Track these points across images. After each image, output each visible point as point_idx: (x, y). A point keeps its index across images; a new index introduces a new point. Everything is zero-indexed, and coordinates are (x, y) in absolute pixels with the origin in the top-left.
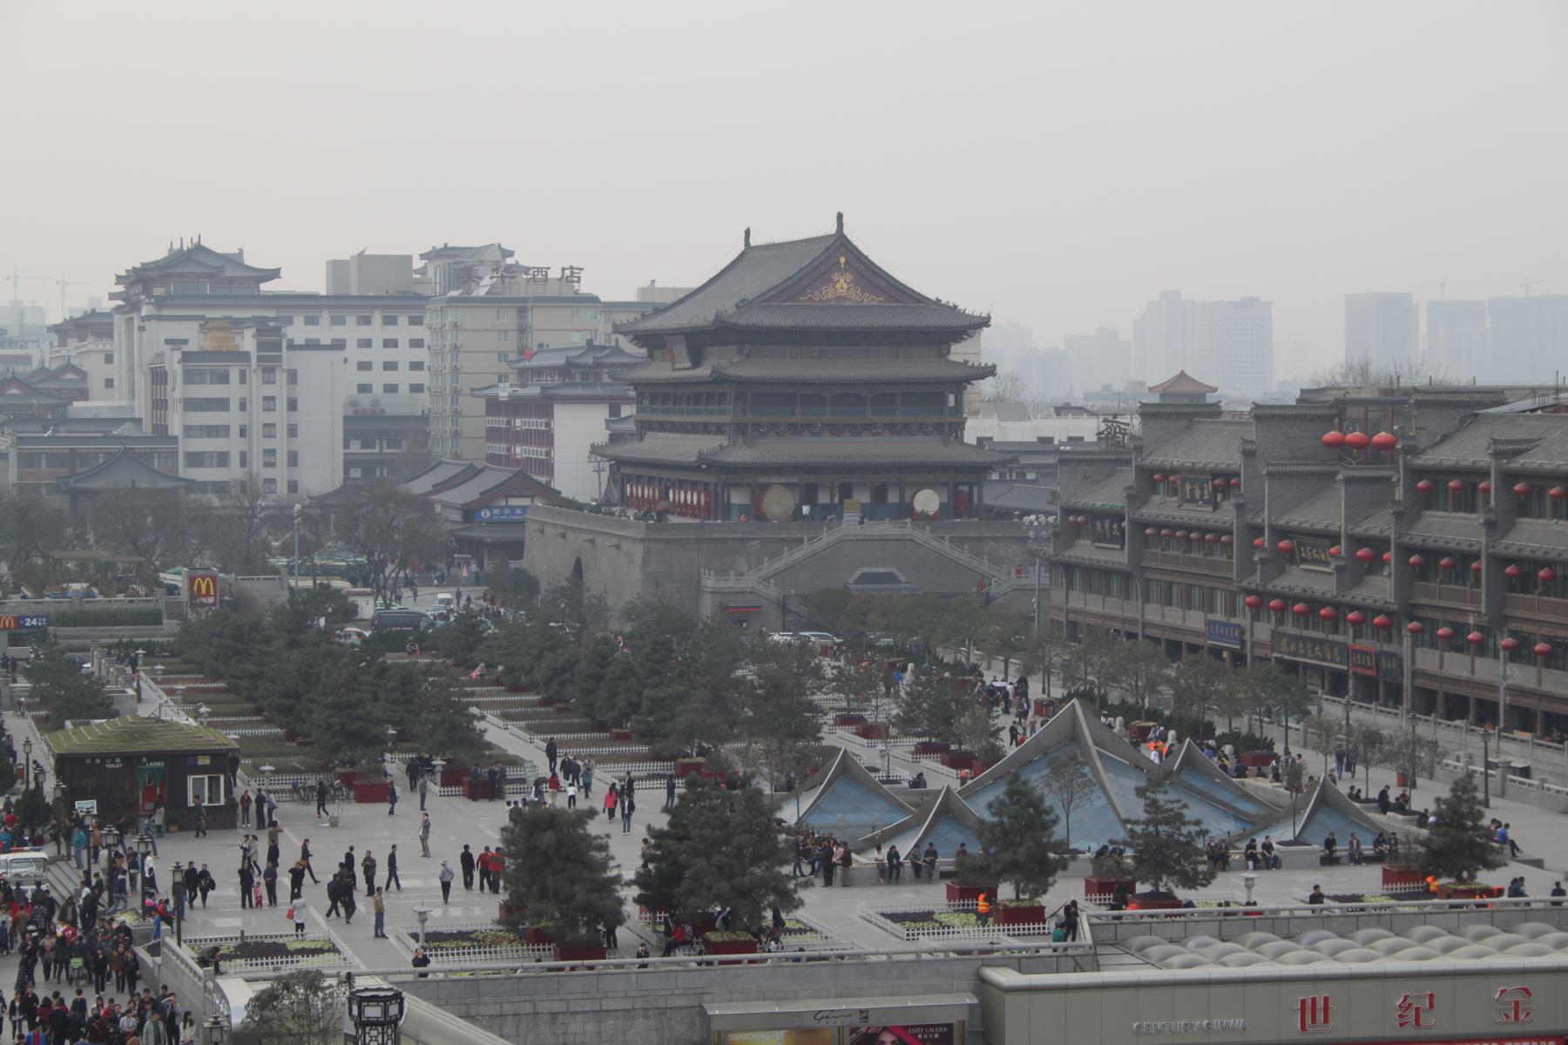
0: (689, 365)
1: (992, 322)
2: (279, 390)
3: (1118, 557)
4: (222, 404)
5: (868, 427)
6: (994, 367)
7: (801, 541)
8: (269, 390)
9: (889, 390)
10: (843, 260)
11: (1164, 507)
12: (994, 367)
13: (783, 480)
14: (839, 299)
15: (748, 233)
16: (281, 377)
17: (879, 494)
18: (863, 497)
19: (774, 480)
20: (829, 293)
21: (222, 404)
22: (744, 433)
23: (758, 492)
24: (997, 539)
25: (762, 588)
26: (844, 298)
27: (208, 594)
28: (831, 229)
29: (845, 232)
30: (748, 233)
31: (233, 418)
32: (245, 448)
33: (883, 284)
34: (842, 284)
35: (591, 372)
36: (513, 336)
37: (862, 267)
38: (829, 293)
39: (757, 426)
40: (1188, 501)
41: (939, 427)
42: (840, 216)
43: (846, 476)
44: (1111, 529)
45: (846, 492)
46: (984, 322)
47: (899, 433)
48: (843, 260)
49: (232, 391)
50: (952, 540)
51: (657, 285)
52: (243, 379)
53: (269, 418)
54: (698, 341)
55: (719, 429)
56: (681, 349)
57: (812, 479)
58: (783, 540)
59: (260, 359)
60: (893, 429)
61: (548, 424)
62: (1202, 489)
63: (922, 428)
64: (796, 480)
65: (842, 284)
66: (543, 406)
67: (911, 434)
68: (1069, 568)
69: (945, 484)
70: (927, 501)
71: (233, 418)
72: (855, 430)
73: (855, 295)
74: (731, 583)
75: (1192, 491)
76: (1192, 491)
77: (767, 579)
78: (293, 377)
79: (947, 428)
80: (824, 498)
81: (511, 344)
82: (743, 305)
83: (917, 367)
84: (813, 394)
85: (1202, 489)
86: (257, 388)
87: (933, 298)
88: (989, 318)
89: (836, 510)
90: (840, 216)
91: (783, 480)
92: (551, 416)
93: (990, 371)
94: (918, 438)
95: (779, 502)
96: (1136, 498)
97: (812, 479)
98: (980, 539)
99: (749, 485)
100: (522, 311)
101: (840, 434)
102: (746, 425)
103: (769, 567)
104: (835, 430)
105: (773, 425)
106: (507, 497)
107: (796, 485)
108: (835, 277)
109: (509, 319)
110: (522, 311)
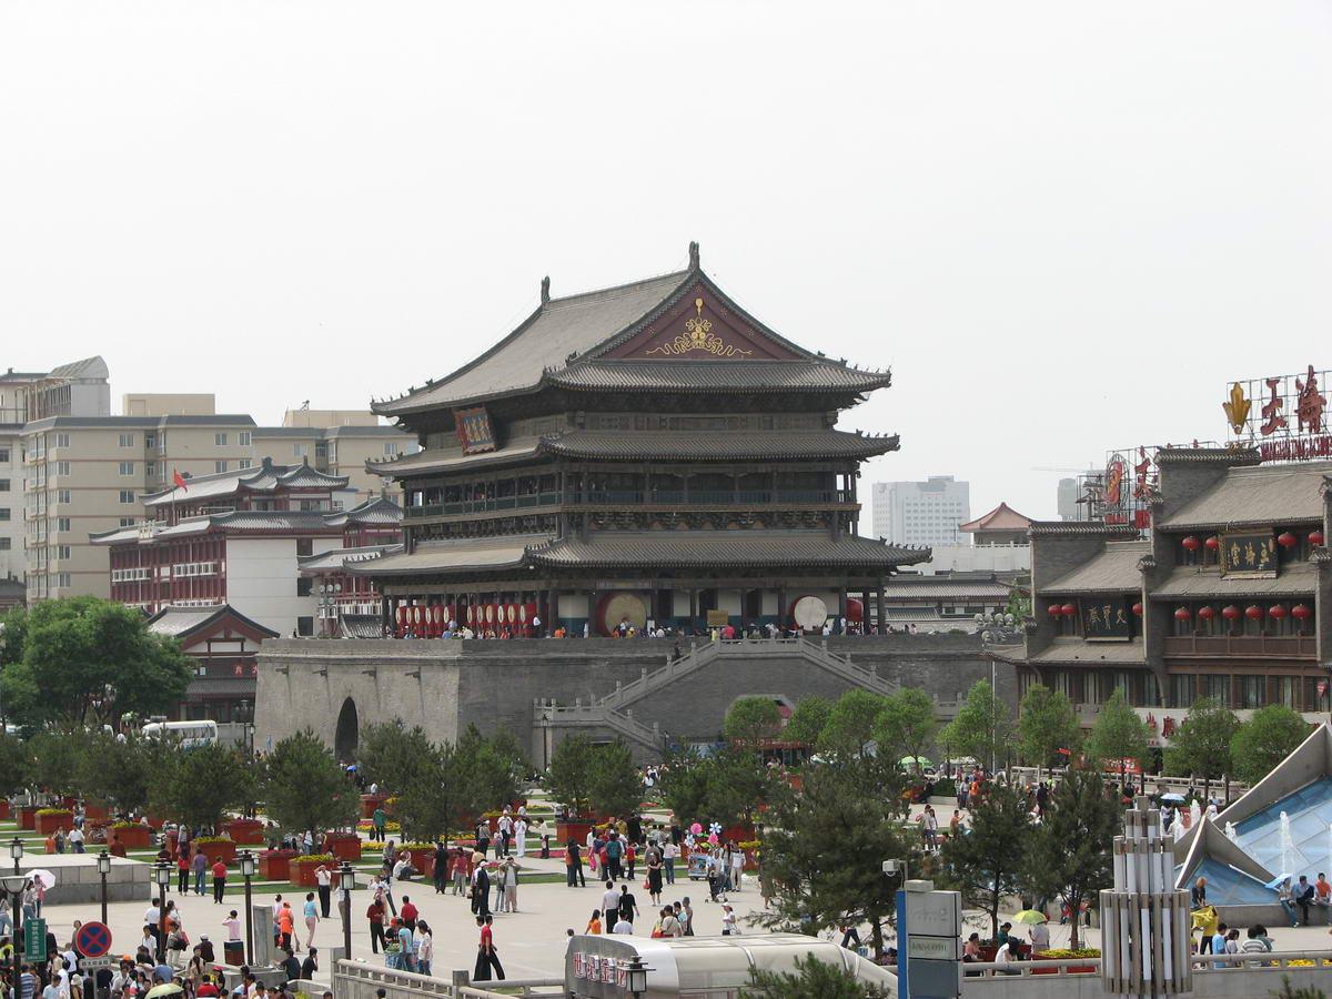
0: (492, 445)
1: (892, 381)
3: (1134, 653)
5: (737, 519)
6: (896, 438)
7: (663, 661)
9: (762, 469)
10: (699, 303)
11: (1190, 583)
12: (896, 438)
13: (630, 586)
14: (695, 352)
15: (546, 284)
17: (752, 603)
18: (731, 607)
20: (682, 346)
22: (579, 526)
23: (600, 603)
24: (908, 658)
25: (617, 722)
28: (682, 263)
29: (702, 267)
30: (546, 284)
33: (751, 334)
34: (699, 334)
35: (272, 502)
36: (140, 469)
37: (723, 312)
38: (682, 346)
39: (596, 516)
40: (1234, 569)
41: (826, 518)
42: (694, 248)
43: (709, 580)
44: (1113, 616)
45: (709, 600)
46: (883, 381)
47: (775, 526)
48: (699, 303)
50: (855, 659)
51: (312, 407)
54: (504, 412)
55: (542, 524)
56: (478, 429)
57: (667, 584)
58: (640, 661)
60: (767, 520)
61: (216, 568)
62: (1258, 550)
63: (805, 519)
64: (646, 585)
65: (699, 334)
66: (211, 545)
67: (790, 526)
68: (1049, 672)
69: (834, 590)
70: (812, 612)
72: (718, 522)
73: (716, 347)
74: (578, 715)
75: (1242, 555)
76: (1242, 555)
77: (623, 710)
79: (836, 518)
80: (681, 609)
81: (137, 478)
82: (574, 362)
83: (792, 439)
84: (666, 476)
85: (1258, 550)
87: (815, 352)
88: (889, 375)
89: (696, 627)
90: (694, 248)
91: (630, 586)
92: (223, 555)
93: (889, 444)
95: (627, 611)
96: (1156, 572)
97: (667, 584)
98: (888, 657)
99: (585, 593)
100: (151, 438)
101: (699, 528)
102: (581, 515)
103: (624, 694)
104: (693, 521)
105: (616, 514)
106: (210, 641)
107: (645, 592)
108: (690, 324)
109: (137, 449)
110: (151, 438)
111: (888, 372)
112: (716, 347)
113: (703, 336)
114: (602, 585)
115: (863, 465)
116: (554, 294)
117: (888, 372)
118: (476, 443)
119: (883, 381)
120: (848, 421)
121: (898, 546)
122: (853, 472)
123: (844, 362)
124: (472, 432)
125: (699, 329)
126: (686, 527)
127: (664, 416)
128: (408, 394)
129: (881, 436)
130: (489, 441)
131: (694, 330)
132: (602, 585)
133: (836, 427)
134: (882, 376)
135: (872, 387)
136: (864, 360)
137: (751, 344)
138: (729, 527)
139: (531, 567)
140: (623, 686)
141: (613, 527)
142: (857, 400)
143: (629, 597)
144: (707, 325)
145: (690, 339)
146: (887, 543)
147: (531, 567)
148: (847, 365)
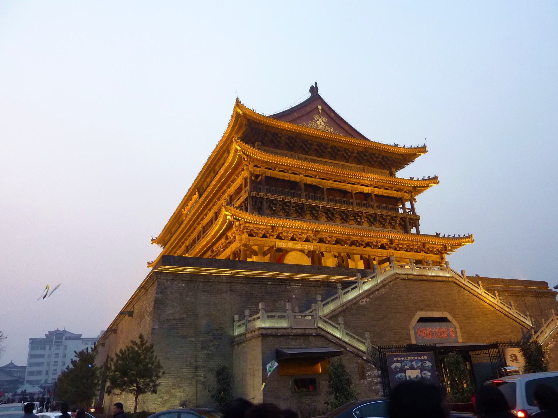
2: (61, 351)
4: (42, 356)
6: (436, 178)
8: (58, 351)
10: (320, 107)
12: (436, 178)
16: (62, 348)
21: (42, 356)
29: (320, 92)
31: (45, 360)
32: (48, 369)
33: (347, 128)
39: (271, 202)
46: (423, 149)
49: (46, 352)
52: (50, 349)
53: (56, 360)
59: (55, 342)
71: (45, 360)
78: (66, 348)
86: (54, 350)
108: (316, 117)
111: (425, 145)
117: (425, 145)
119: (423, 149)
120: (403, 174)
121: (448, 236)
125: (320, 120)
126: (326, 220)
131: (318, 120)
138: (350, 223)
141: (281, 214)
144: (325, 120)
146: (441, 236)
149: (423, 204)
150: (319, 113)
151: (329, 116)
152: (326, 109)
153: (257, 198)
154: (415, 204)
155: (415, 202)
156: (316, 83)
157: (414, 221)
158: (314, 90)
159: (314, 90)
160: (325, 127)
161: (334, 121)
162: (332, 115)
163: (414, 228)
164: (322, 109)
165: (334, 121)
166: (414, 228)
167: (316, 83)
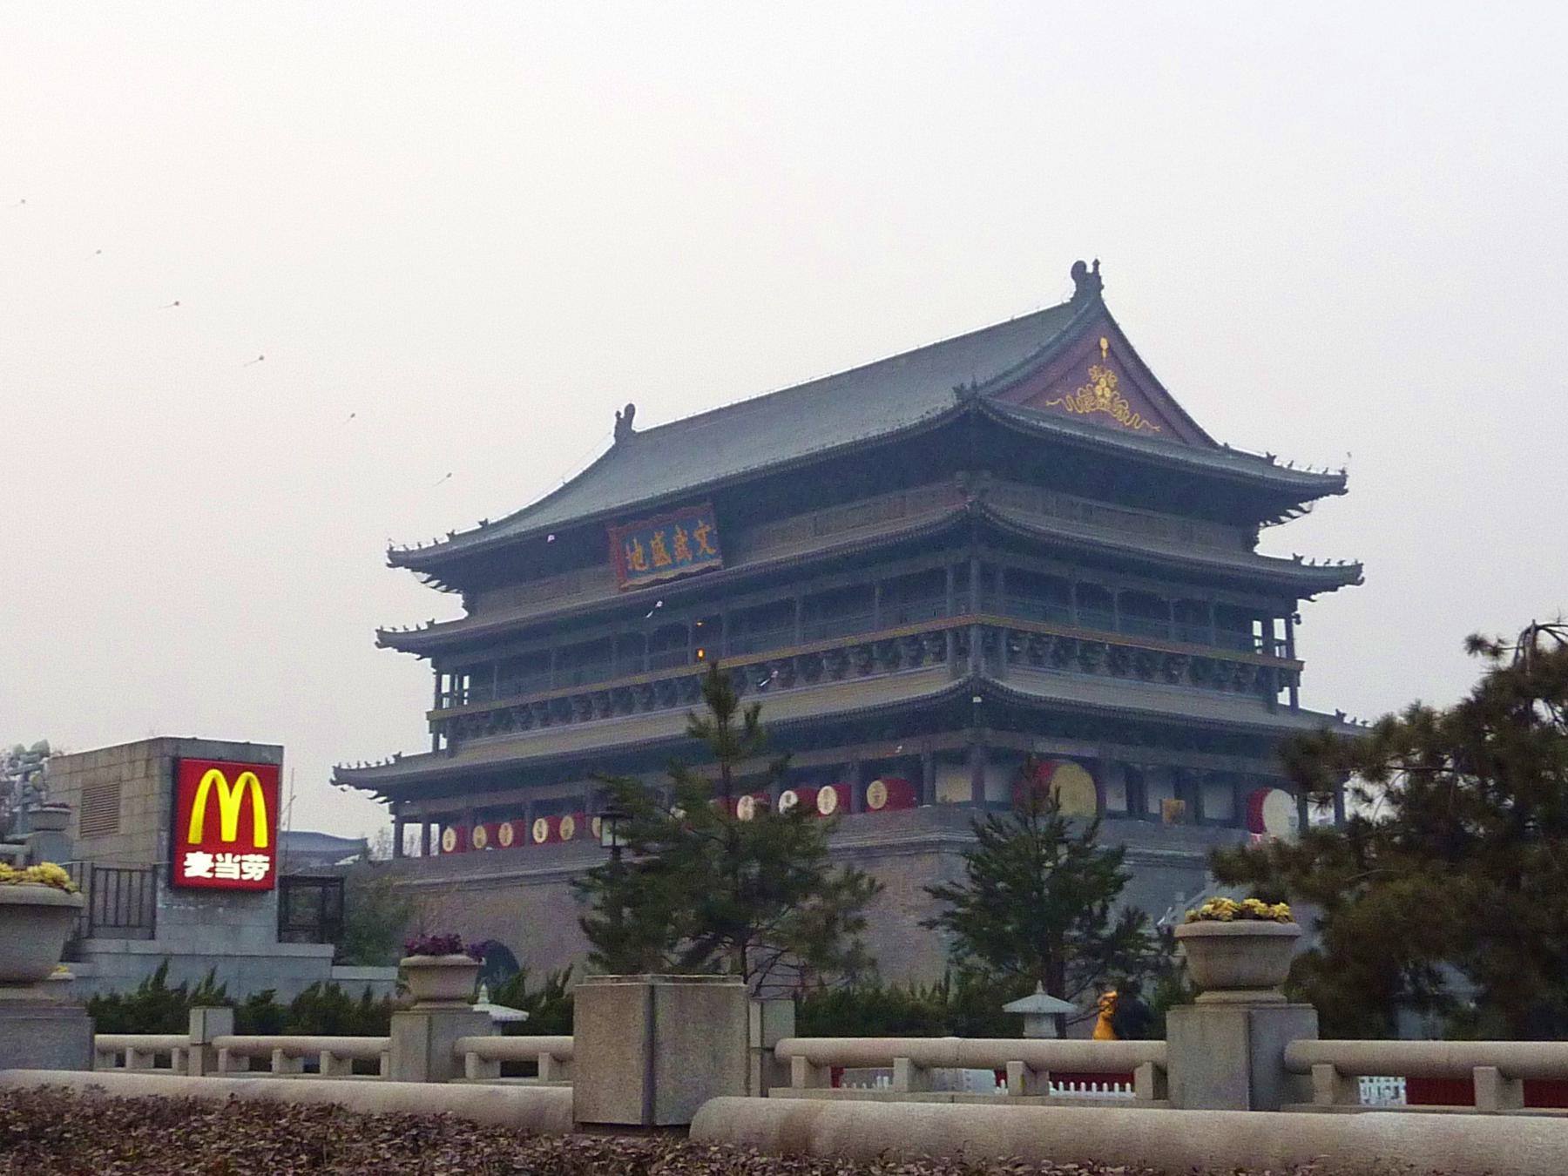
6: (1358, 567)
10: (1104, 344)
12: (1358, 567)
15: (630, 410)
19: (1062, 748)
26: (1105, 415)
27: (244, 844)
28: (1063, 291)
30: (630, 410)
46: (1335, 485)
48: (1104, 344)
64: (1090, 751)
65: (1104, 389)
94: (1230, 694)
104: (1120, 661)
108: (1094, 372)
111: (1343, 472)
112: (1123, 415)
113: (1108, 393)
114: (1044, 746)
115: (1302, 603)
116: (639, 425)
117: (1343, 472)
118: (653, 569)
119: (1335, 485)
120: (1274, 542)
122: (1291, 618)
123: (1271, 458)
124: (648, 555)
125: (1103, 382)
127: (1075, 499)
128: (447, 540)
129: (1334, 564)
130: (712, 557)
131: (1097, 383)
132: (1044, 746)
133: (1258, 550)
134: (1335, 477)
135: (1316, 497)
136: (1299, 454)
137: (1159, 415)
139: (977, 700)
140: (1187, 898)
142: (1294, 513)
143: (1076, 767)
145: (1094, 395)
147: (977, 700)
148: (1276, 463)
149: (1318, 627)
150: (1100, 362)
151: (1124, 372)
152: (1118, 349)
153: (990, 627)
154: (1295, 626)
155: (1299, 622)
156: (1096, 264)
157: (1290, 674)
158: (1087, 280)
159: (1087, 280)
160: (1112, 401)
161: (1130, 379)
162: (1130, 365)
163: (1287, 689)
164: (1110, 349)
165: (1134, 383)
166: (1287, 689)
167: (1096, 264)
